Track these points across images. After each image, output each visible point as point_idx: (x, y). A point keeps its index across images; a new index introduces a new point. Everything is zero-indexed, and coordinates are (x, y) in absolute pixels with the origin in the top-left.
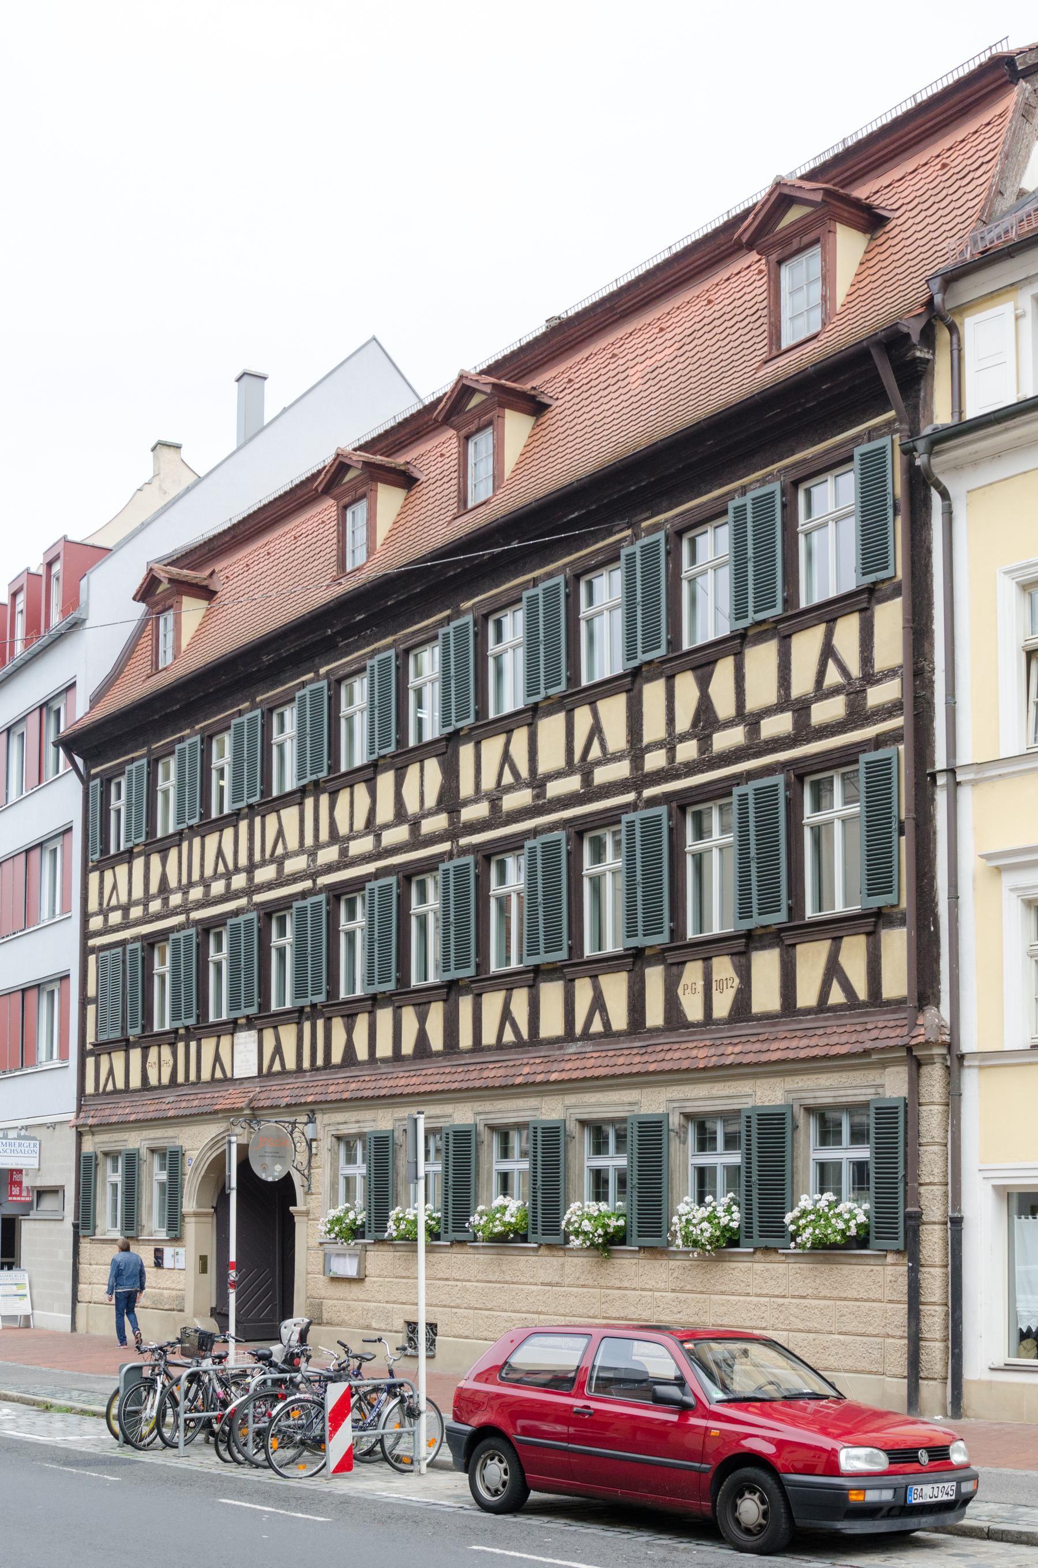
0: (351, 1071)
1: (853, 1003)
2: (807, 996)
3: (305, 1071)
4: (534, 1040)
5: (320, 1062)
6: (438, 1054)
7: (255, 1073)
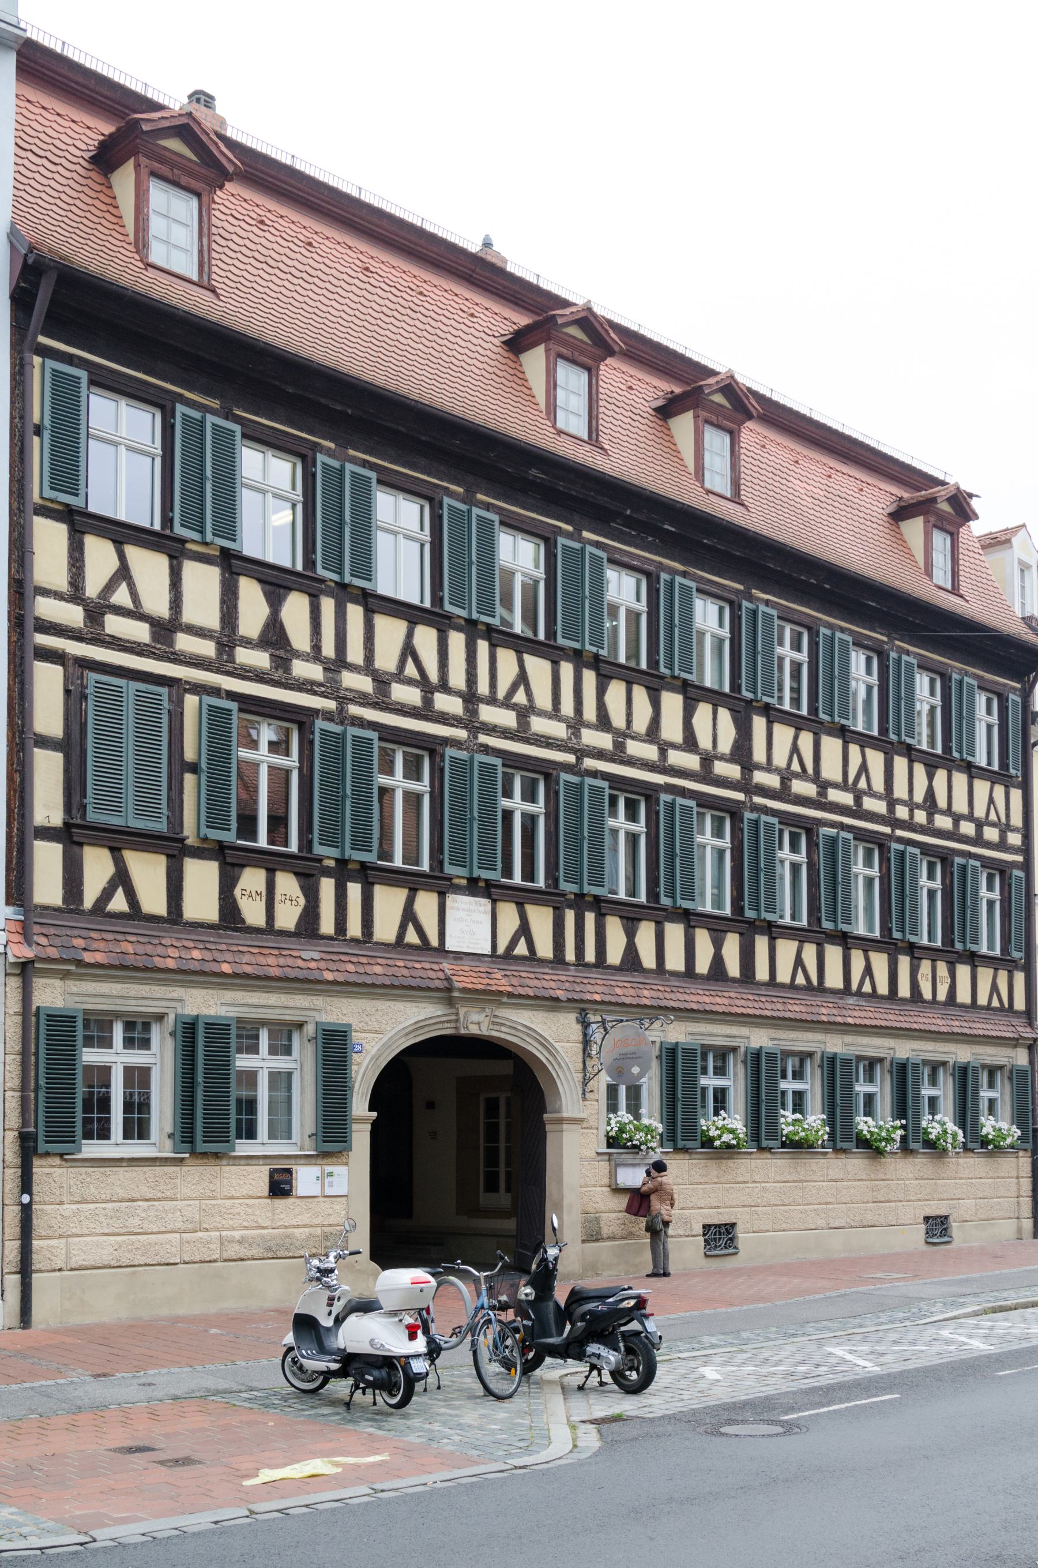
0: (633, 976)
1: (1002, 1009)
2: (982, 1000)
3: (568, 964)
4: (821, 989)
5: (590, 956)
6: (734, 980)
7: (487, 950)
